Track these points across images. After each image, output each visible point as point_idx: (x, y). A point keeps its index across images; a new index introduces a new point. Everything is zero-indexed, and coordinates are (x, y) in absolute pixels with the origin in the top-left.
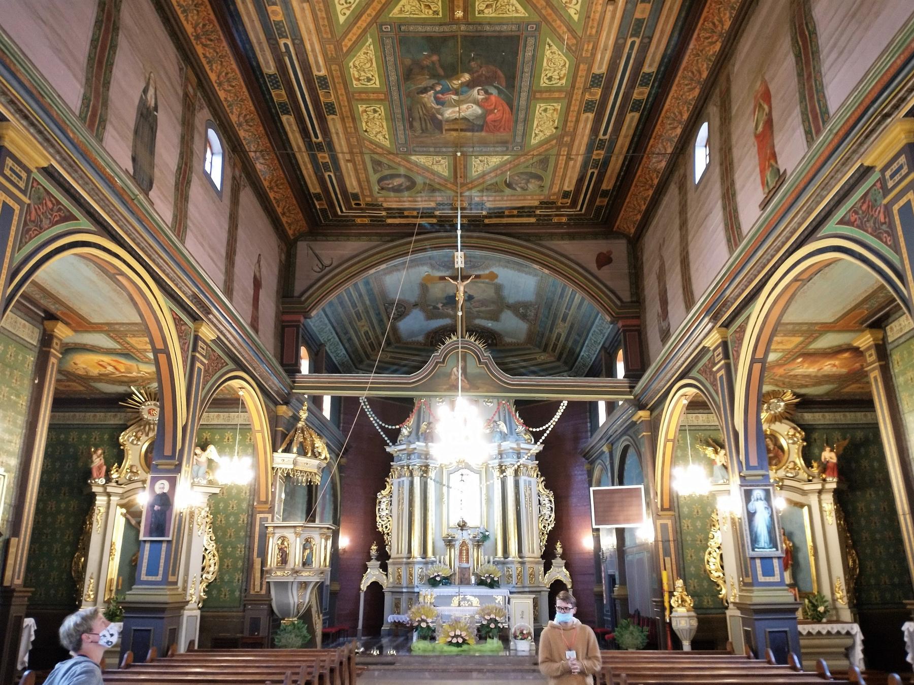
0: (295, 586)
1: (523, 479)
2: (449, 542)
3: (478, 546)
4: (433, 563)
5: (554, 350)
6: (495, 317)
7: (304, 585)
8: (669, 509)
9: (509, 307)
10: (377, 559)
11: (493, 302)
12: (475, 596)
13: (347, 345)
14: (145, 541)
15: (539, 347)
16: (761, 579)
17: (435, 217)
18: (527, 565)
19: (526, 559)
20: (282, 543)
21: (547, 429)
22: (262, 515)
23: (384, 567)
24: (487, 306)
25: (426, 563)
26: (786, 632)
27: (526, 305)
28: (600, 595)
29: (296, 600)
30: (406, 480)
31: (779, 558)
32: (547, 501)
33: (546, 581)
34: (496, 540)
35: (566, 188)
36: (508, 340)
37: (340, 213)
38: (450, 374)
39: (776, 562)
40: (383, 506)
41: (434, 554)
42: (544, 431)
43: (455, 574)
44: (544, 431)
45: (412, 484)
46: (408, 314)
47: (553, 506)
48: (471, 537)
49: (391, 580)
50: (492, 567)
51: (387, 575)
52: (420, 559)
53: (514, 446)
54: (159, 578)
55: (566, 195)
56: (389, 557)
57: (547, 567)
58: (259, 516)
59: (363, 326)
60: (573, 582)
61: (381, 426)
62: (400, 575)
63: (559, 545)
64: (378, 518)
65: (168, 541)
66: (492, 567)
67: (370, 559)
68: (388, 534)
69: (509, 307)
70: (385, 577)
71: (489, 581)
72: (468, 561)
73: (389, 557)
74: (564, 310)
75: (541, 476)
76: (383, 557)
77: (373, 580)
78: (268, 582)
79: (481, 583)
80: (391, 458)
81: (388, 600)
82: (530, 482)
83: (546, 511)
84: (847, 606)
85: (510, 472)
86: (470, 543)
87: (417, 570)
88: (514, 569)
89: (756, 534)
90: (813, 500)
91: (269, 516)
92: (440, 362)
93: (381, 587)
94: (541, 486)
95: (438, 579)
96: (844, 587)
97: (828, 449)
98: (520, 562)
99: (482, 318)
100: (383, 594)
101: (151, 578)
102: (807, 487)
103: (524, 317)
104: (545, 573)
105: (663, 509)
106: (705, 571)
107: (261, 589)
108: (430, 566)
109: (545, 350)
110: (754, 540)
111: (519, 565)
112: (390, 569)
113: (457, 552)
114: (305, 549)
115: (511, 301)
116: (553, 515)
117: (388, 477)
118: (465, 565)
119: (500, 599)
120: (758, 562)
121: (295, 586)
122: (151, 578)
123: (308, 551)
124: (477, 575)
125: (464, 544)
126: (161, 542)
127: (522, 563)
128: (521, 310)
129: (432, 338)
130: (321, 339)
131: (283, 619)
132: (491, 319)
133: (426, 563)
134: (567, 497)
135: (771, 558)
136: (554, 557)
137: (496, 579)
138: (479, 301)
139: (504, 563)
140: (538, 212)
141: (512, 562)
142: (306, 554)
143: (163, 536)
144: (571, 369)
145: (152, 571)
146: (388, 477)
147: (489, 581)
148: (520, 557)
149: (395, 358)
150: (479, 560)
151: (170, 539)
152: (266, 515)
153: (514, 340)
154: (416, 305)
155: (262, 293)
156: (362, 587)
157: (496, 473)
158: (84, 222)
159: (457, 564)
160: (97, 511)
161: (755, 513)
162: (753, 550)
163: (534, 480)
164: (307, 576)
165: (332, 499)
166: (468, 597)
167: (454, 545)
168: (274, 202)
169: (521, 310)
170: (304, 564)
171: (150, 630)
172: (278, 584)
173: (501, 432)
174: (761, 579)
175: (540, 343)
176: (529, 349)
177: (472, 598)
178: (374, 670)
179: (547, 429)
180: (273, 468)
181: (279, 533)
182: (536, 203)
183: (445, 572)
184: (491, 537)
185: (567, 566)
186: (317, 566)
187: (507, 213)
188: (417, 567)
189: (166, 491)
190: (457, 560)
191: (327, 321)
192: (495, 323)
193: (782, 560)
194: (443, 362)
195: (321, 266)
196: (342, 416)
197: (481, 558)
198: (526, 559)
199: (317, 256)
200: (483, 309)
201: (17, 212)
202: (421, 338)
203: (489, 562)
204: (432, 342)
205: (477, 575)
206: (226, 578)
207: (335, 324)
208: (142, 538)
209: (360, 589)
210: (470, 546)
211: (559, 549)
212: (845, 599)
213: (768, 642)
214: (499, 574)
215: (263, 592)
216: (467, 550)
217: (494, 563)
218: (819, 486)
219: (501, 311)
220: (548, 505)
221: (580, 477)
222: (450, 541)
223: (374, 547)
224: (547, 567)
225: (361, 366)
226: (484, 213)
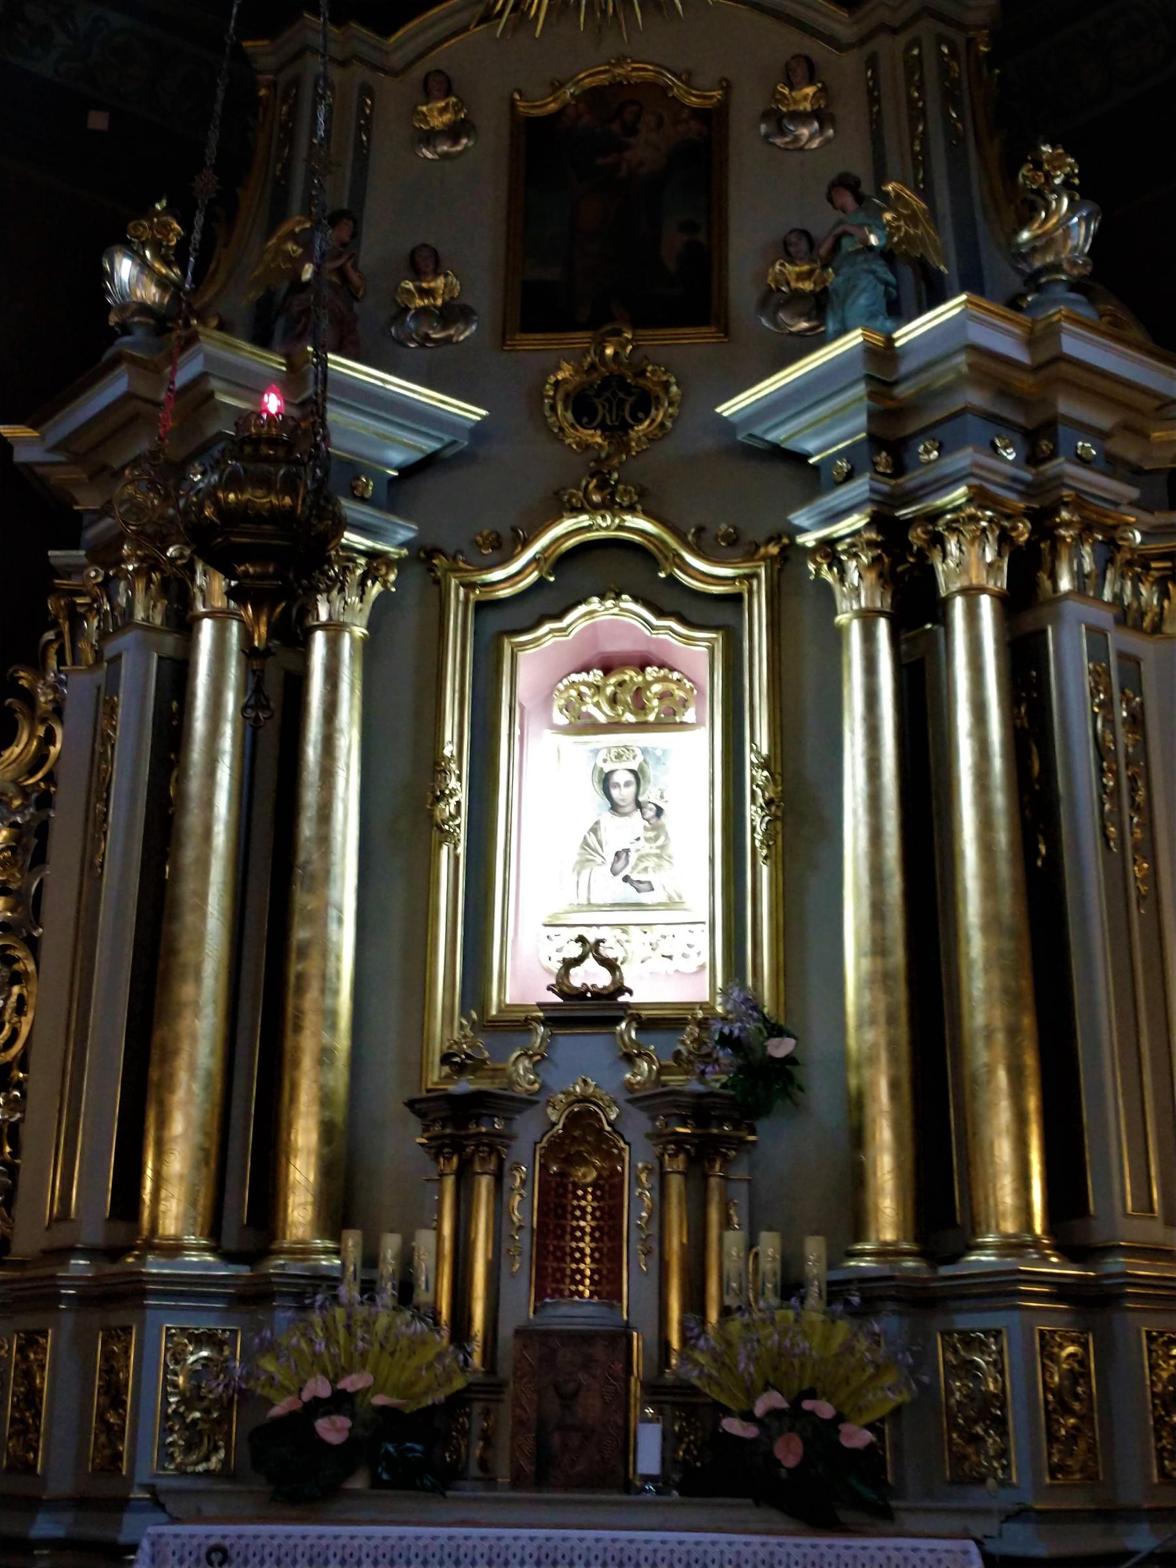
2: (463, 1125)
3: (702, 1156)
4: (316, 1287)
18: (1139, 1324)
19: (1116, 1264)
25: (253, 1298)
34: (857, 1104)
41: (340, 1208)
43: (489, 1388)
50: (817, 1331)
52: (199, 1260)
53: (1004, 340)
62: (31, 1398)
66: (817, 1331)
71: (789, 1452)
72: (608, 1285)
79: (715, 1471)
82: (1131, 664)
85: (968, 567)
86: (638, 1125)
87: (170, 1357)
88: (1018, 1359)
95: (332, 1430)
98: (1062, 1290)
108: (283, 1316)
111: (1052, 1317)
113: (523, 1207)
118: (580, 1308)
124: (681, 1402)
125: (583, 1119)
127: (1090, 1302)
133: (253, 1298)
137: (856, 1437)
139: (921, 1301)
141: (1000, 1289)
147: (789, 1452)
148: (1072, 1252)
150: (688, 1283)
157: (855, 592)
159: (521, 1305)
167: (495, 1146)
183: (403, 1368)
184: (819, 1093)
188: (164, 1323)
190: (520, 1267)
197: (727, 1247)
198: (1116, 1264)
203: (791, 1287)
205: (681, 1402)
210: (636, 1158)
214: (887, 1396)
216: (609, 1191)
217: (835, 1291)
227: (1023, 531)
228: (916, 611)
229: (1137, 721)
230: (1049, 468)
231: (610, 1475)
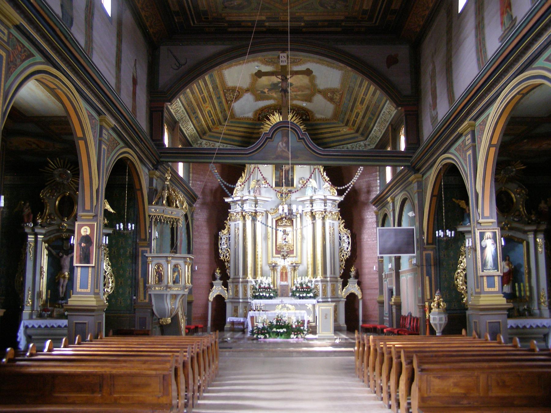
0: (168, 297)
1: (328, 222)
5: (354, 124)
6: (309, 99)
7: (174, 297)
8: (432, 244)
9: (320, 92)
10: (221, 279)
11: (308, 89)
12: (292, 305)
13: (195, 122)
14: (77, 267)
15: (343, 122)
16: (486, 289)
17: (265, 26)
20: (158, 268)
21: (348, 187)
22: (143, 249)
23: (225, 285)
24: (302, 91)
26: (499, 322)
27: (333, 91)
28: (381, 303)
29: (169, 306)
30: (240, 223)
31: (498, 276)
32: (346, 237)
33: (343, 294)
35: (364, 7)
36: (318, 116)
37: (192, 25)
38: (277, 147)
39: (496, 279)
40: (223, 241)
42: (346, 189)
44: (346, 189)
45: (244, 225)
46: (241, 97)
47: (350, 241)
48: (290, 263)
49: (231, 294)
51: (227, 290)
54: (89, 290)
55: (365, 12)
56: (229, 278)
58: (141, 249)
59: (207, 107)
60: (363, 294)
61: (226, 186)
63: (352, 269)
64: (220, 250)
65: (92, 267)
67: (214, 279)
68: (228, 261)
69: (320, 92)
70: (226, 292)
73: (229, 278)
74: (362, 96)
75: (342, 219)
76: (225, 278)
77: (218, 293)
78: (150, 295)
80: (228, 206)
81: (229, 308)
82: (333, 224)
83: (345, 245)
84: (547, 308)
89: (485, 260)
90: (531, 237)
91: (148, 249)
92: (269, 138)
93: (224, 299)
96: (546, 295)
97: (543, 202)
99: (298, 100)
100: (225, 304)
101: (83, 290)
102: (527, 228)
103: (331, 100)
105: (428, 244)
106: (454, 285)
107: (145, 298)
109: (346, 125)
110: (484, 264)
112: (230, 286)
114: (174, 272)
115: (321, 87)
117: (227, 220)
118: (285, 283)
119: (310, 306)
120: (485, 278)
121: (168, 297)
122: (83, 290)
123: (176, 274)
125: (284, 268)
126: (88, 267)
128: (329, 95)
129: (260, 114)
130: (176, 118)
131: (161, 319)
132: (306, 101)
135: (494, 276)
136: (350, 277)
138: (296, 87)
140: (343, 24)
142: (175, 276)
143: (89, 263)
144: (366, 140)
145: (84, 285)
146: (227, 220)
149: (230, 130)
151: (93, 265)
152: (146, 249)
153: (323, 117)
154: (247, 91)
155: (138, 88)
156: (209, 298)
158: (38, 57)
160: (29, 246)
161: (486, 247)
162: (483, 271)
163: (336, 223)
164: (175, 290)
165: (186, 236)
166: (287, 305)
167: (276, 269)
168: (144, 18)
169: (329, 95)
170: (174, 282)
171: (85, 323)
172: (156, 295)
173: (312, 187)
174: (486, 289)
175: (343, 119)
176: (335, 123)
177: (290, 306)
178: (226, 351)
179: (348, 187)
180: (149, 216)
181: (156, 261)
182: (342, 18)
185: (359, 284)
186: (183, 283)
187: (320, 24)
189: (88, 233)
191: (181, 105)
192: (309, 104)
193: (500, 278)
194: (271, 138)
195: (178, 65)
196: (191, 175)
199: (174, 56)
200: (299, 93)
201: (5, 58)
202: (250, 115)
204: (259, 118)
206: (121, 291)
207: (187, 106)
208: (75, 264)
209: (208, 300)
212: (547, 303)
213: (488, 329)
215: (147, 300)
216: (286, 273)
218: (534, 228)
219: (313, 95)
220: (347, 240)
221: (370, 220)
222: (274, 267)
223: (218, 271)
224: (345, 284)
225: (205, 137)
226: (303, 24)
228: (313, 217)
229: (334, 229)
231: (287, 296)
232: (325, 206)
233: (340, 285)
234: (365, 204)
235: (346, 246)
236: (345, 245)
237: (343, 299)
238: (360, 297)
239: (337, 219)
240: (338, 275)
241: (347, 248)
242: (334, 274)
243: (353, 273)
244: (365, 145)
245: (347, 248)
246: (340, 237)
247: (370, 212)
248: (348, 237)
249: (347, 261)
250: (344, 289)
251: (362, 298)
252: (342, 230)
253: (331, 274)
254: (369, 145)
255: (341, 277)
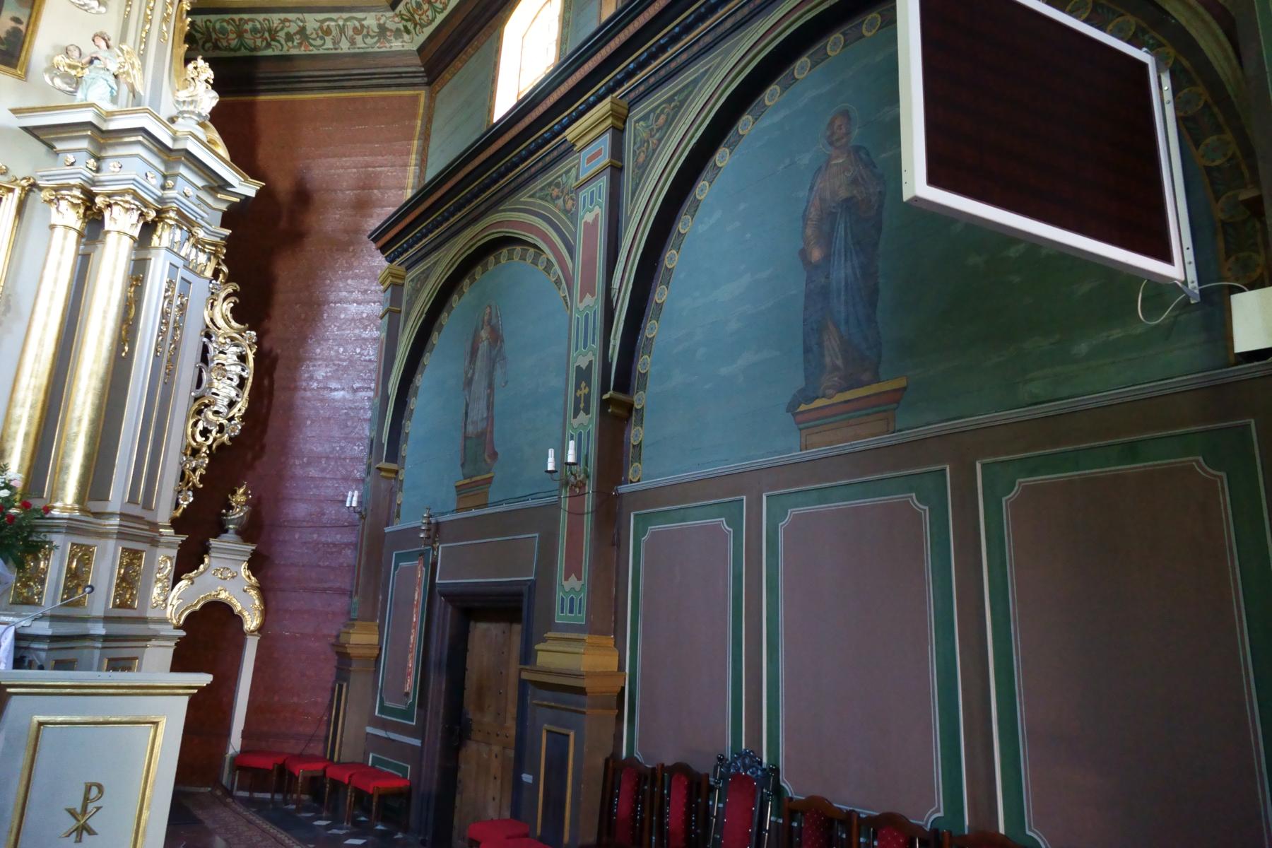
47: (249, 374)
57: (188, 562)
60: (266, 613)
63: (240, 497)
75: (228, 280)
83: (224, 390)
85: (122, 222)
94: (224, 308)
104: (177, 580)
116: (242, 405)
134: (298, 361)
136: (220, 529)
163: (200, 287)
185: (256, 565)
211: (238, 511)
221: (353, 308)
224: (188, 562)
227: (152, 215)
229: (182, 308)
230: (170, 194)
232: (163, 188)
233: (165, 560)
234: (344, 245)
235: (228, 391)
236: (224, 390)
237: (168, 630)
238: (252, 622)
239: (209, 273)
240: (164, 513)
241: (232, 404)
242: (147, 505)
243: (238, 511)
244: (383, 29)
245: (232, 404)
246: (205, 350)
247: (356, 277)
248: (242, 358)
249: (218, 454)
250: (183, 584)
251: (260, 629)
252: (220, 322)
253: (133, 499)
254: (397, 34)
255: (176, 524)
